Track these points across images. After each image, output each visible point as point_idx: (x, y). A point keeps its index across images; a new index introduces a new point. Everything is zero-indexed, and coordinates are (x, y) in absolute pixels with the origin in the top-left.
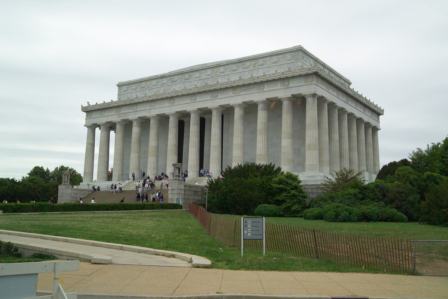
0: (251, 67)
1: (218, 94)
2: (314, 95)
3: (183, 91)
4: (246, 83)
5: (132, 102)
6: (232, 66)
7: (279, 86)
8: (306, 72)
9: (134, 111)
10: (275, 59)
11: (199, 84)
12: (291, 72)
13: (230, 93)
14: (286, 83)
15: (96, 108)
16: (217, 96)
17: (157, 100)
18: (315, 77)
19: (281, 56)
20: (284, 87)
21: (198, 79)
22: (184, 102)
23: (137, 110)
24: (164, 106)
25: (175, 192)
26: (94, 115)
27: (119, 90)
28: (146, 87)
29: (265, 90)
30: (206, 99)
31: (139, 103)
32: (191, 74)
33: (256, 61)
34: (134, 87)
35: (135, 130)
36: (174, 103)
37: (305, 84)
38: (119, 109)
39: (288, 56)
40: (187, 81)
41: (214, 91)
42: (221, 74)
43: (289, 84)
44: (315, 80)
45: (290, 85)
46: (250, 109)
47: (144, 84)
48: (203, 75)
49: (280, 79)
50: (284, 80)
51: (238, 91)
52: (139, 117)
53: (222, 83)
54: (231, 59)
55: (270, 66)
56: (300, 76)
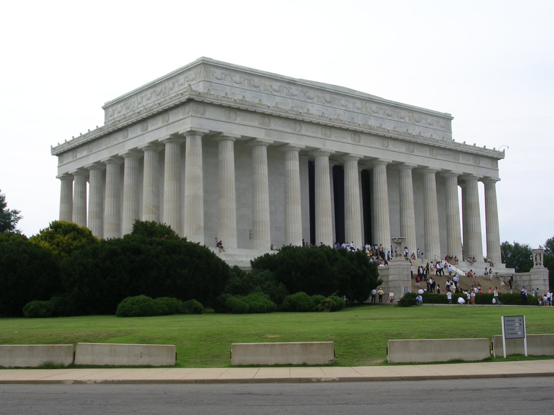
0: (407, 119)
3: (379, 129)
5: (300, 118)
6: (386, 108)
7: (471, 161)
9: (295, 132)
11: (402, 129)
12: (487, 151)
13: (426, 152)
16: (413, 151)
17: (340, 129)
19: (435, 118)
21: (344, 108)
22: (374, 146)
24: (345, 140)
28: (262, 88)
30: (401, 150)
31: (311, 123)
32: (334, 96)
34: (237, 78)
36: (359, 141)
38: (266, 120)
40: (329, 105)
42: (374, 114)
47: (256, 81)
54: (385, 98)
55: (426, 126)
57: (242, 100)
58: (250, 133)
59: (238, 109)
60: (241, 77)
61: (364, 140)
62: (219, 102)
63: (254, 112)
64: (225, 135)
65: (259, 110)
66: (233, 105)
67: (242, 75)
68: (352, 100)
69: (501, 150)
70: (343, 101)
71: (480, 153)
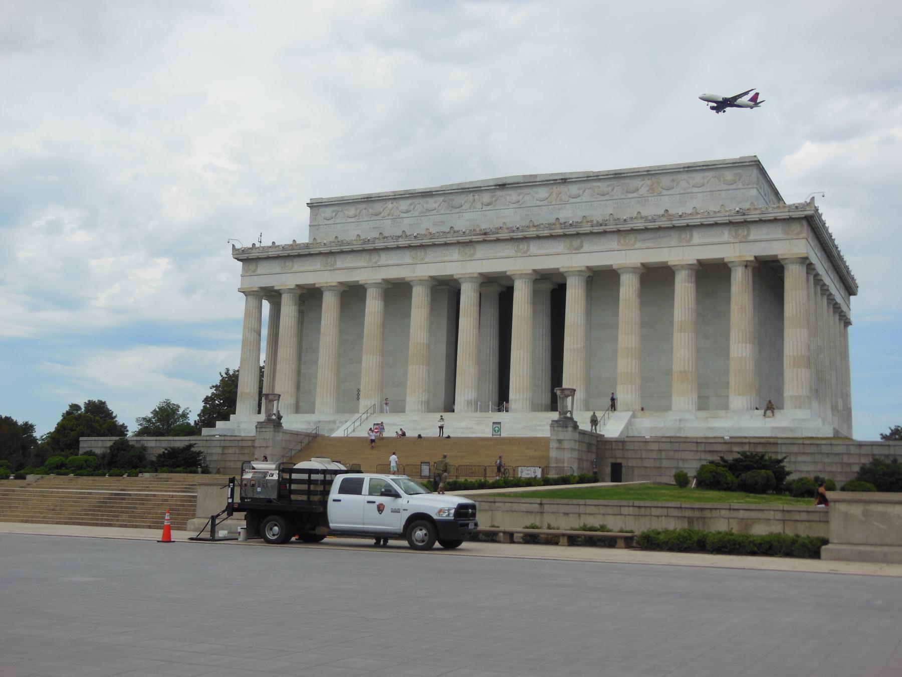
0: (643, 191)
1: (582, 243)
2: (805, 261)
4: (650, 225)
6: (598, 184)
7: (725, 235)
8: (791, 214)
10: (698, 177)
13: (613, 243)
14: (742, 232)
15: (272, 253)
16: (581, 247)
17: (434, 245)
18: (805, 223)
19: (711, 174)
20: (738, 240)
21: (515, 206)
22: (500, 254)
23: (380, 263)
25: (566, 445)
26: (263, 268)
27: (313, 216)
29: (692, 243)
30: (554, 251)
31: (386, 249)
32: (499, 193)
33: (654, 180)
34: (352, 211)
35: (373, 305)
36: (472, 255)
37: (786, 237)
38: (330, 260)
39: (729, 175)
40: (488, 208)
41: (571, 235)
42: (572, 200)
43: (748, 234)
44: (804, 231)
45: (752, 237)
46: (656, 278)
47: (378, 207)
48: (527, 198)
49: (731, 223)
50: (740, 224)
51: (632, 238)
52: (383, 280)
53: (595, 222)
55: (688, 191)
56: (775, 220)
57: (291, 245)
58: (308, 279)
59: (289, 257)
60: (356, 209)
61: (481, 251)
62: (265, 255)
63: (310, 255)
64: (276, 288)
65: (313, 251)
66: (280, 253)
67: (358, 206)
68: (530, 190)
69: (808, 201)
70: (512, 195)
71: (739, 218)
